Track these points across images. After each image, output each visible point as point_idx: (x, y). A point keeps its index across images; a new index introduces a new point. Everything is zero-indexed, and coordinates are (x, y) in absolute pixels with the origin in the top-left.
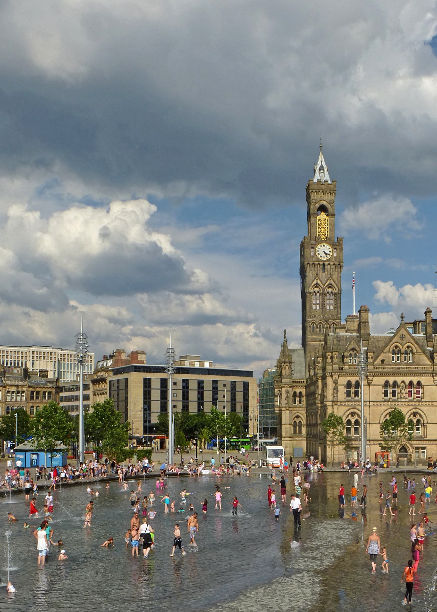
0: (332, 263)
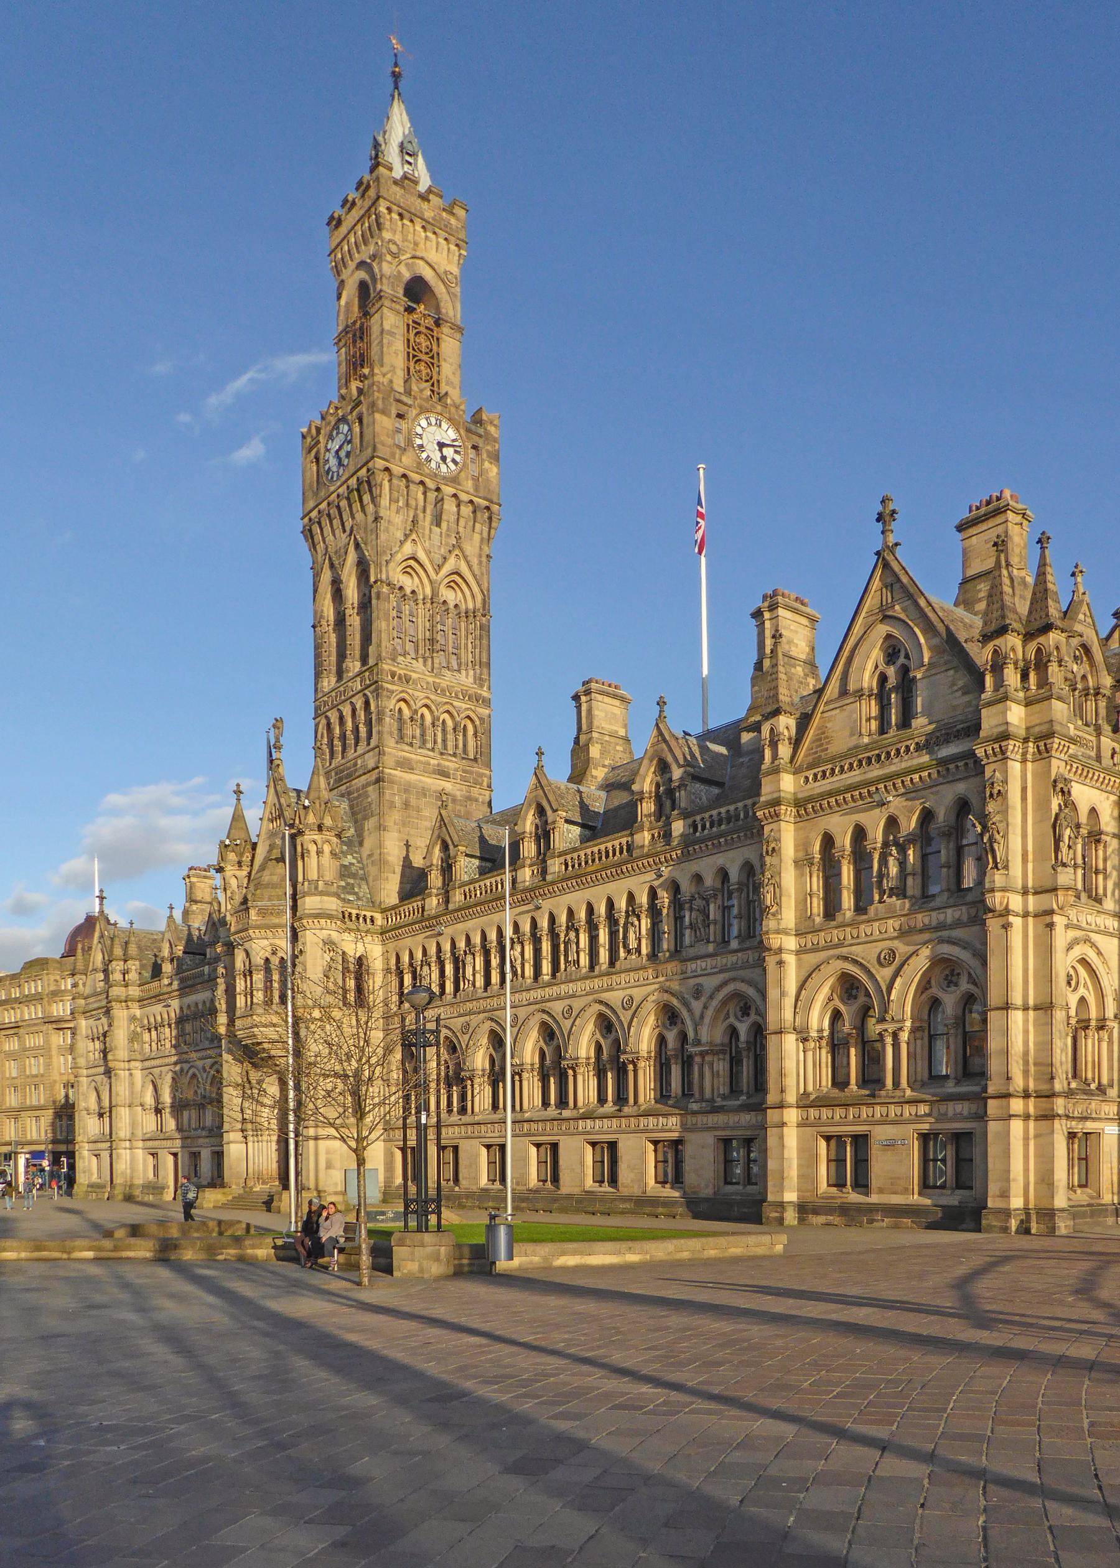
0: (464, 497)
